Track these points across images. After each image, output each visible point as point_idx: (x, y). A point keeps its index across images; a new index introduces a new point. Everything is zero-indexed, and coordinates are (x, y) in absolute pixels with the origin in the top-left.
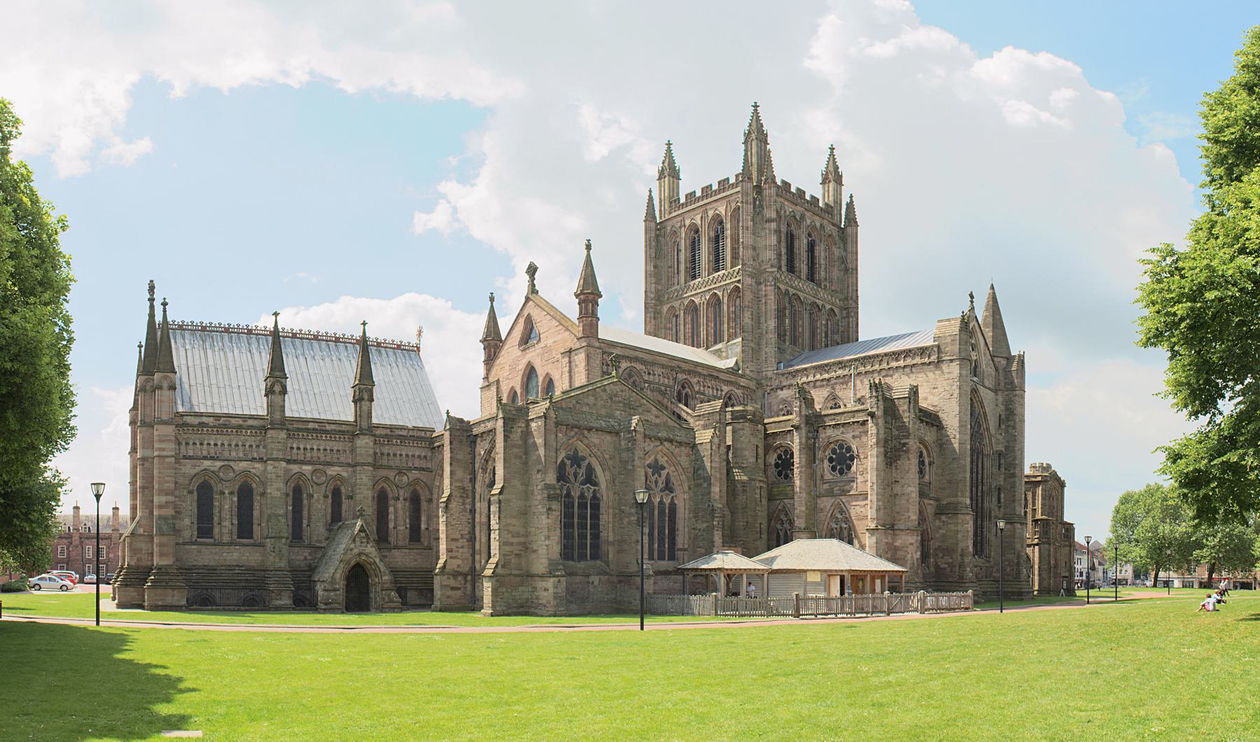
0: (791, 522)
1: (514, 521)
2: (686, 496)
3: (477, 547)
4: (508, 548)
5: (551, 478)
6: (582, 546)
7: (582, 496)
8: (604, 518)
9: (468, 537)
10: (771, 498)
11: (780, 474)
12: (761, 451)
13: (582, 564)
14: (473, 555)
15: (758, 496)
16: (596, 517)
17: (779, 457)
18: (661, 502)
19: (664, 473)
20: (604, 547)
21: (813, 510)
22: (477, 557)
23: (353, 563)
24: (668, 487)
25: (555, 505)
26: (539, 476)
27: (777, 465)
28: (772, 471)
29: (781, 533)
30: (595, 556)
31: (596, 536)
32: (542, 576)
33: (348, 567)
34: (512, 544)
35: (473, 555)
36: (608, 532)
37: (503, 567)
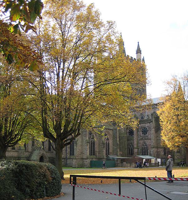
0: (133, 146)
1: (80, 147)
2: (111, 141)
3: (67, 152)
4: (78, 153)
5: (87, 139)
6: (92, 152)
7: (91, 142)
8: (96, 146)
9: (65, 150)
10: (128, 140)
11: (130, 134)
12: (126, 129)
13: (92, 156)
14: (66, 154)
15: (125, 140)
16: (94, 146)
17: (130, 130)
18: (106, 143)
19: (107, 136)
20: (96, 153)
21: (138, 143)
22: (67, 155)
23: (41, 155)
24: (108, 139)
25: (89, 144)
26: (85, 138)
27: (129, 132)
28: (128, 133)
29: (131, 149)
30: (94, 155)
31: (94, 150)
32: (86, 159)
33: (40, 157)
34: (79, 152)
35: (66, 154)
36: (97, 149)
37: (77, 157)
